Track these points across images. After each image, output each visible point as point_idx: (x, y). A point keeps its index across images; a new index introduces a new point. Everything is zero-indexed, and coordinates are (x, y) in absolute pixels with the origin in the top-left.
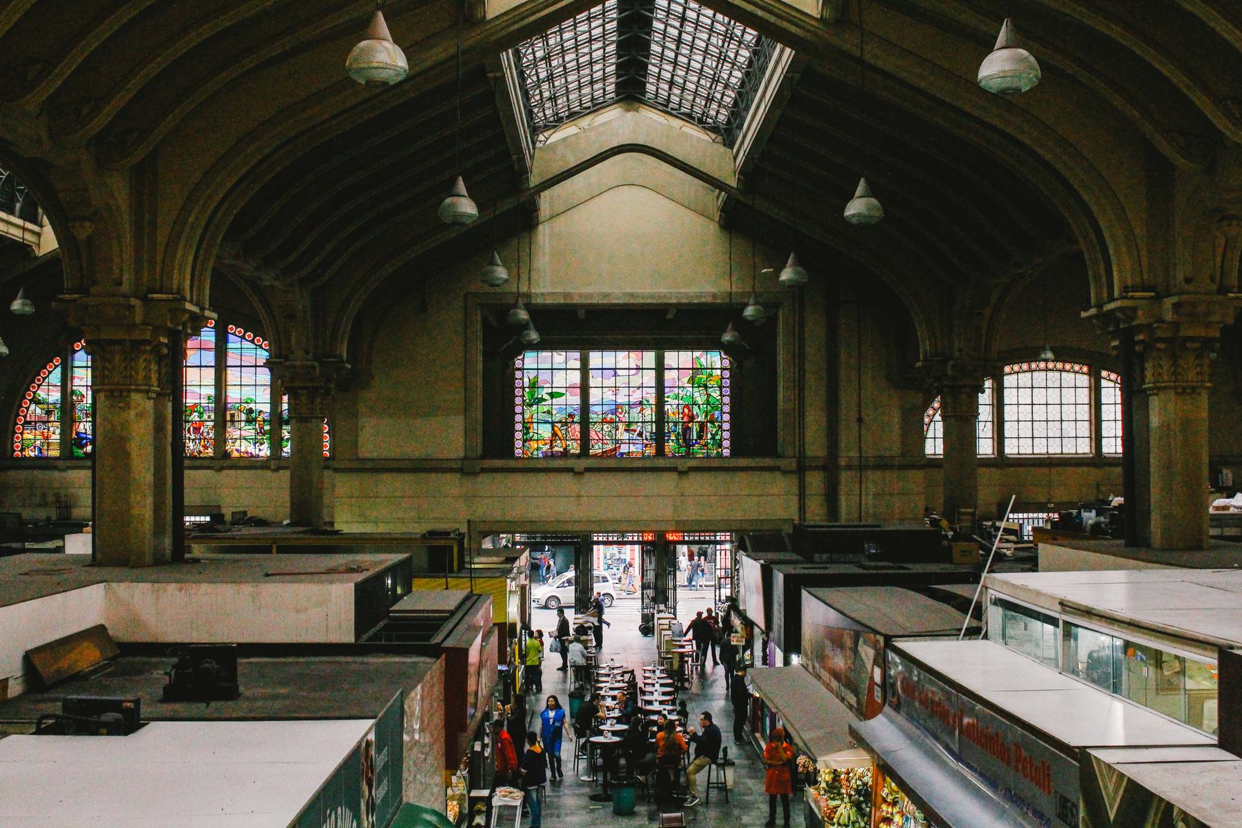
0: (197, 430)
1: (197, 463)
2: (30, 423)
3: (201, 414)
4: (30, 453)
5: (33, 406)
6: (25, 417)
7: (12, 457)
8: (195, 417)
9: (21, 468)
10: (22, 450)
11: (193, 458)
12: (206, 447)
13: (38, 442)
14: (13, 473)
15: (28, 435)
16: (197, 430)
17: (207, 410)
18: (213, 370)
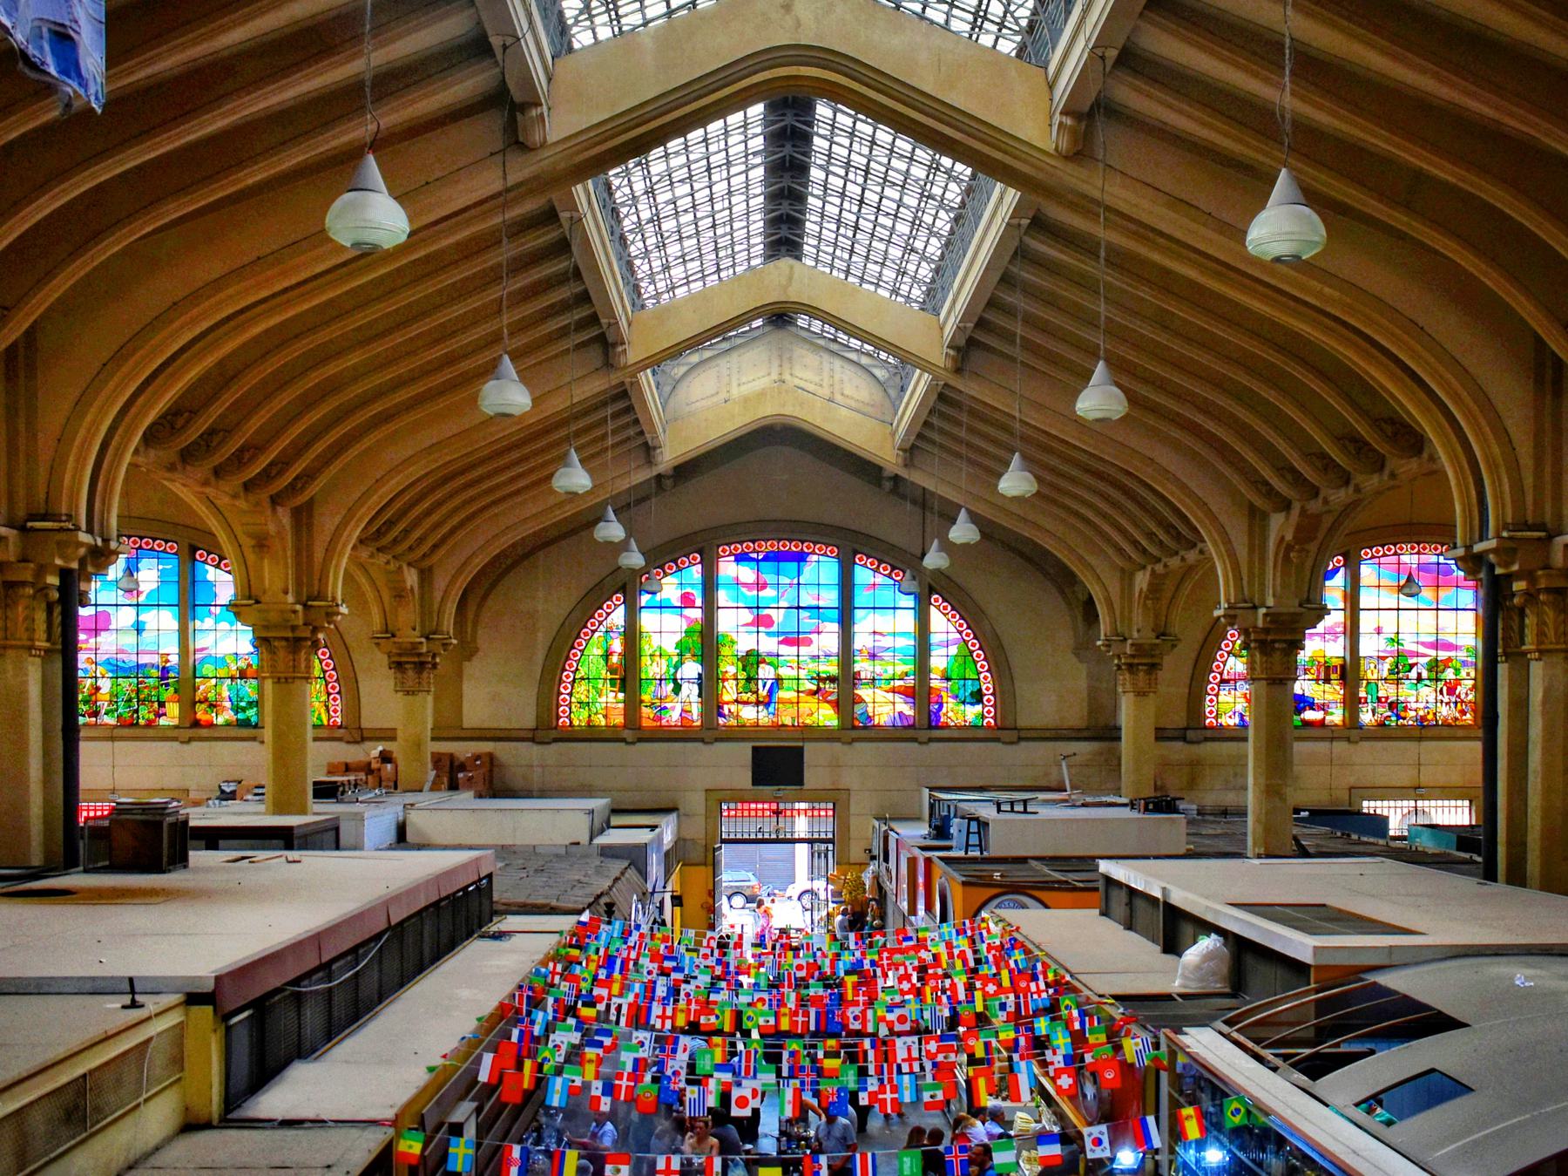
0: (1451, 691)
2: (1227, 681)
3: (1457, 670)
4: (1230, 721)
6: (1221, 674)
7: (1205, 728)
8: (1449, 674)
9: (1213, 739)
10: (1216, 718)
14: (1209, 746)
16: (1451, 691)
17: (1464, 664)
18: (1471, 614)
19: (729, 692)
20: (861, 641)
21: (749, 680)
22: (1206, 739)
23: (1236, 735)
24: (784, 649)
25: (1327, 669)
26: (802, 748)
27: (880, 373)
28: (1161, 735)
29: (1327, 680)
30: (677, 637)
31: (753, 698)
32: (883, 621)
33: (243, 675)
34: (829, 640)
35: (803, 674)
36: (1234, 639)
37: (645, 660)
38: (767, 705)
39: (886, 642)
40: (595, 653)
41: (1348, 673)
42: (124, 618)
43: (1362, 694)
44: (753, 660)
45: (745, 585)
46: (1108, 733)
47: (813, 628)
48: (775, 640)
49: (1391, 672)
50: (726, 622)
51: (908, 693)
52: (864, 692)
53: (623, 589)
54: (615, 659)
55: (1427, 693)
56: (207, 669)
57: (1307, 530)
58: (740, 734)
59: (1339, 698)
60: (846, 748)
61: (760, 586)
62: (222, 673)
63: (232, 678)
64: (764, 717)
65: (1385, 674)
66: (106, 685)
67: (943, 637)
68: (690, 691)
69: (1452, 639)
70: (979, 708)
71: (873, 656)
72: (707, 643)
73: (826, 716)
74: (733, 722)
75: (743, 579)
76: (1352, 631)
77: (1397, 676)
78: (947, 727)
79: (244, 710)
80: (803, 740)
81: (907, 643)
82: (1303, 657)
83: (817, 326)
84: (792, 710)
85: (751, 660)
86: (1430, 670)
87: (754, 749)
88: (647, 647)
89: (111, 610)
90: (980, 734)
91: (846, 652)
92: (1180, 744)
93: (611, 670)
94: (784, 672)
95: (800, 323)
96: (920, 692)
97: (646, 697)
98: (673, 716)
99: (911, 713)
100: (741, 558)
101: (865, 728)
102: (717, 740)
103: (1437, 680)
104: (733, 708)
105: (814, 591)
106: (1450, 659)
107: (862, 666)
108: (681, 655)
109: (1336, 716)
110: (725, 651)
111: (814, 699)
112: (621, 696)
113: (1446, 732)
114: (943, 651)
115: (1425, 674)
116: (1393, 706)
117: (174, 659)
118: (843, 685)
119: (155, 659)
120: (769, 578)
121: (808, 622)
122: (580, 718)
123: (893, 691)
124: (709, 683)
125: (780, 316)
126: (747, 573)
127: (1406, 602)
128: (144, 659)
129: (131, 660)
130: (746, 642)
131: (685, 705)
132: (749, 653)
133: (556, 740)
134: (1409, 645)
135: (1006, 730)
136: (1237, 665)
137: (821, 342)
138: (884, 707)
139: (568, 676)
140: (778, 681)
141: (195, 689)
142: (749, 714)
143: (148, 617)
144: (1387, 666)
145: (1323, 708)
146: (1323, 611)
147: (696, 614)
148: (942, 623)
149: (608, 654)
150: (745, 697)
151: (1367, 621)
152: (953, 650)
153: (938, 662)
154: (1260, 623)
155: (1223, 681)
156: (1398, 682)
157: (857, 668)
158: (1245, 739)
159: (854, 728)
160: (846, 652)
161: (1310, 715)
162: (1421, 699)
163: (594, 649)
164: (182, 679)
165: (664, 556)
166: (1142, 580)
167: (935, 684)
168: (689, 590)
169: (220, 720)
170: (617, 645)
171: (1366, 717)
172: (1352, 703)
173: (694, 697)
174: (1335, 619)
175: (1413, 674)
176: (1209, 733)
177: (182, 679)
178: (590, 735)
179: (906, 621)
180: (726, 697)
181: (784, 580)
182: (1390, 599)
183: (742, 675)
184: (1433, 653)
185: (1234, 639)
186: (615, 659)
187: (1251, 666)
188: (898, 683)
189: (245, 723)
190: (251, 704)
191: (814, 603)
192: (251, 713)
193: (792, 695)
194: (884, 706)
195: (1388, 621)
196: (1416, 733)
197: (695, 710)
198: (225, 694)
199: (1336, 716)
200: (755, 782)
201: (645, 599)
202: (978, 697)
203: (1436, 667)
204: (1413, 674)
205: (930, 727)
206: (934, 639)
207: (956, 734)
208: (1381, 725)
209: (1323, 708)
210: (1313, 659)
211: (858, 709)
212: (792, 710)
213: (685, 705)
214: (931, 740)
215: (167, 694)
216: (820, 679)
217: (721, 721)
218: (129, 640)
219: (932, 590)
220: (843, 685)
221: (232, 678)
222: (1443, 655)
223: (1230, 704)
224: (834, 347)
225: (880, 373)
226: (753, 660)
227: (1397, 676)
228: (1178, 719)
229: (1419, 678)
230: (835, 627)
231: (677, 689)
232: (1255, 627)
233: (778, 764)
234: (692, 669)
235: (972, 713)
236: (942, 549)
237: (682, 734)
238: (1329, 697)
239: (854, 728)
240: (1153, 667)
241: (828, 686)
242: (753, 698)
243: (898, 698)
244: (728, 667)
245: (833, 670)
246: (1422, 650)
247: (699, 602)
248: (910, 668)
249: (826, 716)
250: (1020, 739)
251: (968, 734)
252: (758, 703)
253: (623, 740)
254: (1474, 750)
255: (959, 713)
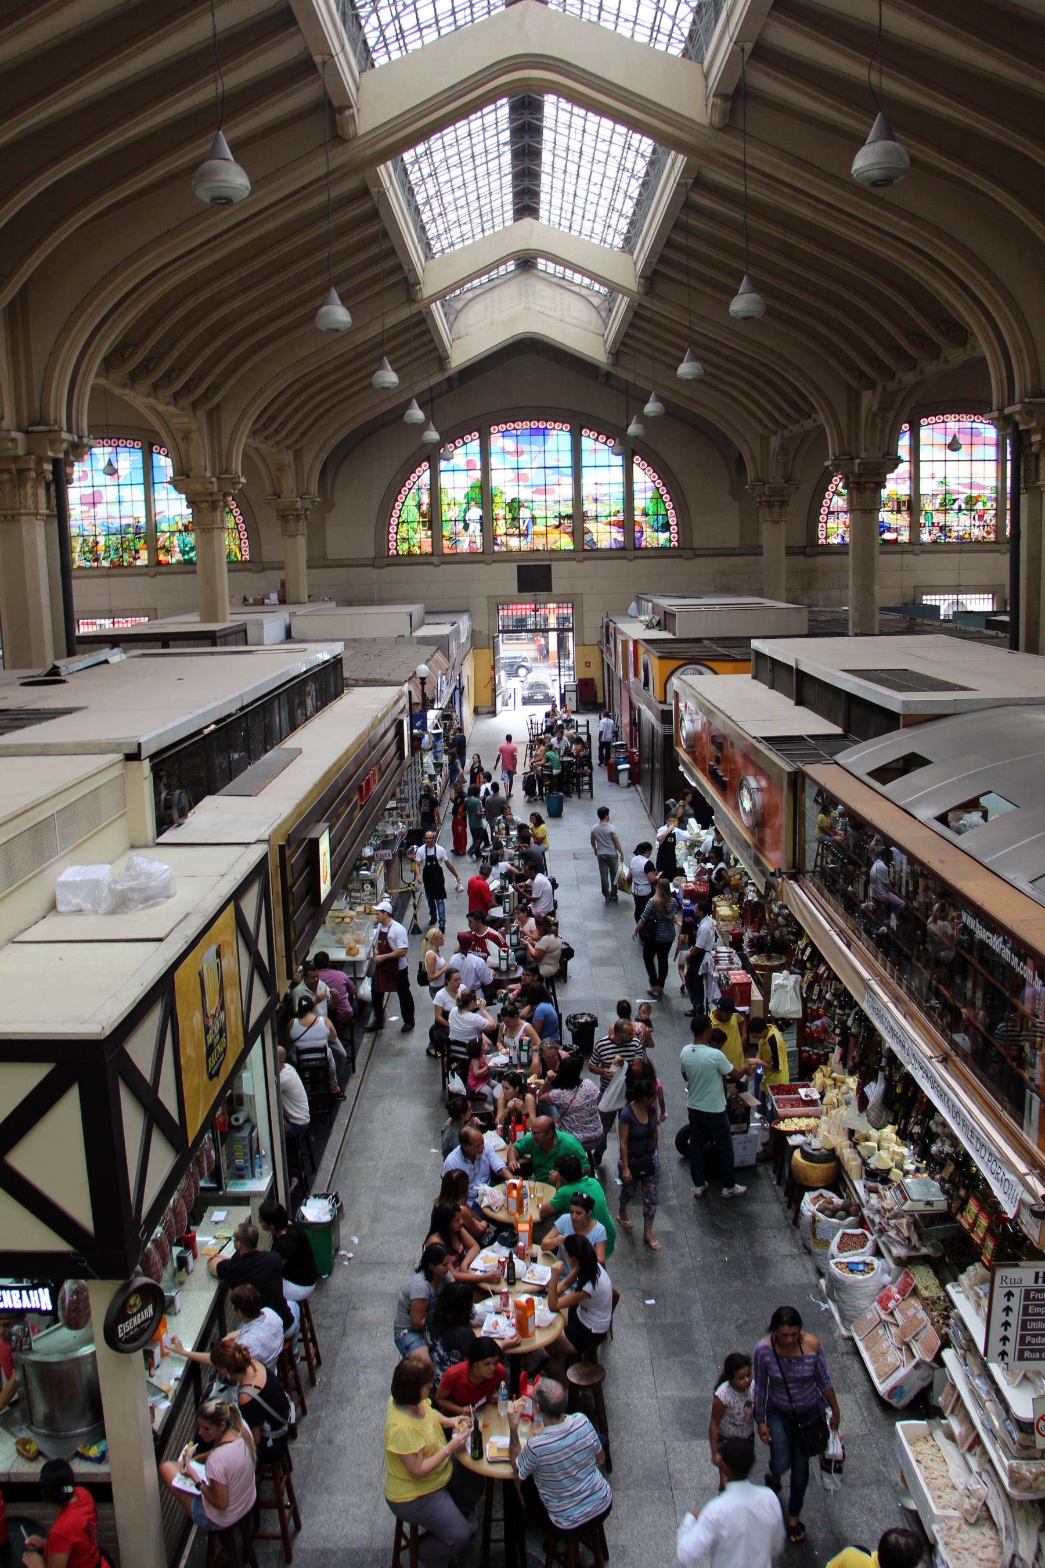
0: (981, 517)
1: (987, 547)
2: (832, 513)
4: (835, 540)
5: (836, 497)
8: (979, 506)
9: (824, 554)
10: (826, 538)
11: (977, 542)
12: (988, 533)
13: (841, 531)
15: (832, 523)
17: (989, 499)
18: (994, 464)
19: (501, 528)
20: (588, 490)
21: (514, 519)
22: (819, 554)
23: (841, 550)
24: (536, 497)
25: (899, 503)
26: (549, 566)
27: (596, 301)
28: (790, 551)
29: (899, 511)
30: (465, 491)
31: (517, 532)
32: (601, 475)
33: (186, 529)
34: (567, 491)
35: (549, 514)
36: (837, 483)
37: (445, 508)
38: (526, 535)
39: (604, 490)
40: (410, 505)
41: (912, 505)
42: (110, 494)
43: (922, 521)
44: (516, 505)
45: (509, 453)
46: (756, 551)
47: (555, 481)
48: (530, 490)
49: (941, 505)
50: (497, 479)
51: (620, 525)
52: (590, 525)
53: (428, 459)
54: (424, 508)
55: (965, 519)
56: (164, 527)
57: (886, 405)
58: (509, 556)
59: (906, 523)
60: (579, 565)
61: (518, 453)
62: (174, 528)
63: (180, 532)
64: (525, 545)
65: (937, 506)
66: (102, 540)
67: (642, 486)
68: (475, 528)
69: (981, 482)
70: (667, 534)
71: (596, 500)
72: (484, 494)
73: (566, 543)
74: (504, 549)
75: (507, 449)
76: (915, 478)
77: (945, 507)
78: (646, 548)
79: (188, 553)
80: (551, 560)
81: (618, 491)
82: (884, 493)
83: (551, 267)
84: (543, 540)
85: (515, 505)
86: (967, 503)
87: (519, 567)
88: (445, 499)
89: (102, 489)
90: (671, 553)
91: (577, 499)
92: (802, 558)
93: (422, 515)
94: (537, 513)
95: (540, 267)
96: (627, 524)
97: (446, 533)
98: (464, 546)
99: (621, 538)
100: (504, 434)
101: (592, 550)
102: (494, 561)
103: (971, 510)
104: (504, 539)
105: (555, 455)
106: (979, 496)
107: (588, 507)
108: (468, 503)
109: (905, 537)
110: (497, 499)
111: (557, 531)
112: (429, 533)
113: (978, 547)
114: (643, 495)
115: (963, 507)
116: (942, 529)
117: (143, 520)
118: (576, 520)
119: (131, 521)
120: (524, 447)
121: (552, 477)
122: (403, 548)
123: (610, 524)
124: (487, 522)
125: (526, 262)
126: (509, 444)
127: (951, 455)
128: (125, 522)
129: (116, 524)
130: (510, 494)
131: (470, 540)
132: (513, 501)
133: (388, 565)
134: (952, 486)
135: (684, 550)
136: (839, 502)
137: (555, 280)
138: (605, 535)
139: (394, 521)
140: (534, 519)
141: (157, 540)
142: (514, 543)
143: (125, 492)
144: (938, 500)
145: (896, 530)
146: (898, 461)
147: (477, 474)
148: (643, 478)
149: (419, 505)
150: (511, 531)
151: (925, 469)
152: (649, 494)
153: (639, 503)
154: (856, 471)
155: (830, 513)
156: (946, 512)
157: (585, 509)
158: (847, 553)
159: (585, 550)
160: (577, 499)
161: (888, 536)
162: (960, 524)
163: (411, 502)
164: (149, 532)
165: (453, 435)
166: (774, 442)
167: (637, 518)
168: (470, 457)
169: (174, 560)
170: (426, 499)
171: (925, 537)
172: (915, 527)
173: (478, 533)
174: (904, 468)
175: (956, 507)
176: (821, 549)
177: (149, 532)
178: (411, 559)
179: (618, 475)
180: (498, 532)
181: (535, 448)
182: (940, 453)
183: (509, 516)
184: (968, 491)
185: (837, 483)
186: (424, 508)
187: (850, 502)
188: (613, 519)
189: (189, 562)
190: (192, 549)
191: (555, 464)
192: (192, 554)
193: (543, 529)
194: (605, 535)
195: (938, 469)
196: (958, 548)
197: (479, 541)
198: (176, 542)
199: (905, 537)
200: (520, 590)
201: (443, 465)
202: (666, 527)
203: (971, 501)
204: (956, 507)
205: (635, 549)
206: (636, 487)
207: (652, 553)
208: (935, 542)
209: (896, 530)
210: (889, 497)
211: (587, 537)
212: (543, 540)
213: (470, 540)
214: (636, 558)
215: (140, 544)
216: (560, 517)
217: (496, 548)
218: (114, 510)
219: (634, 454)
220: (576, 520)
221: (180, 532)
222: (975, 493)
223: (835, 529)
224: (563, 283)
225: (596, 301)
226: (516, 505)
227: (945, 507)
228: (800, 539)
229: (960, 510)
230: (569, 480)
231: (466, 527)
232: (853, 473)
233: (535, 577)
234: (475, 513)
235: (663, 538)
236: (638, 422)
237: (471, 558)
238: (900, 523)
239: (585, 551)
240: (783, 504)
241: (567, 522)
242: (517, 532)
243: (614, 529)
244: (500, 511)
245: (570, 511)
246: (961, 489)
247: (478, 466)
248: (620, 506)
249: (566, 543)
250: (696, 556)
251: (661, 552)
252: (520, 535)
253: (432, 564)
254: (1005, 560)
255: (653, 539)
